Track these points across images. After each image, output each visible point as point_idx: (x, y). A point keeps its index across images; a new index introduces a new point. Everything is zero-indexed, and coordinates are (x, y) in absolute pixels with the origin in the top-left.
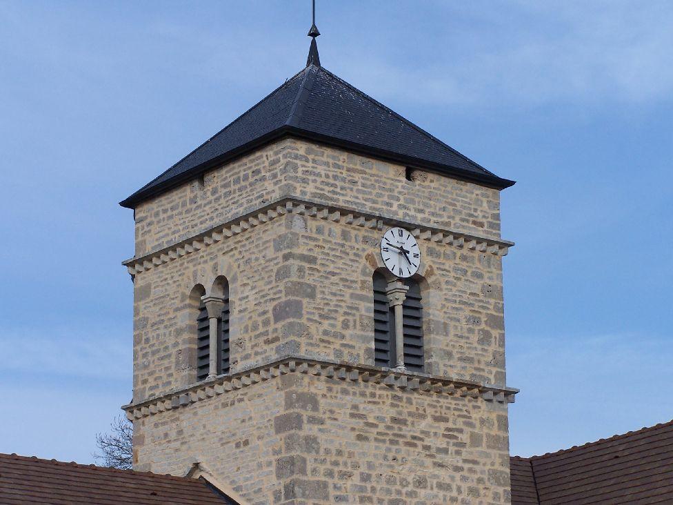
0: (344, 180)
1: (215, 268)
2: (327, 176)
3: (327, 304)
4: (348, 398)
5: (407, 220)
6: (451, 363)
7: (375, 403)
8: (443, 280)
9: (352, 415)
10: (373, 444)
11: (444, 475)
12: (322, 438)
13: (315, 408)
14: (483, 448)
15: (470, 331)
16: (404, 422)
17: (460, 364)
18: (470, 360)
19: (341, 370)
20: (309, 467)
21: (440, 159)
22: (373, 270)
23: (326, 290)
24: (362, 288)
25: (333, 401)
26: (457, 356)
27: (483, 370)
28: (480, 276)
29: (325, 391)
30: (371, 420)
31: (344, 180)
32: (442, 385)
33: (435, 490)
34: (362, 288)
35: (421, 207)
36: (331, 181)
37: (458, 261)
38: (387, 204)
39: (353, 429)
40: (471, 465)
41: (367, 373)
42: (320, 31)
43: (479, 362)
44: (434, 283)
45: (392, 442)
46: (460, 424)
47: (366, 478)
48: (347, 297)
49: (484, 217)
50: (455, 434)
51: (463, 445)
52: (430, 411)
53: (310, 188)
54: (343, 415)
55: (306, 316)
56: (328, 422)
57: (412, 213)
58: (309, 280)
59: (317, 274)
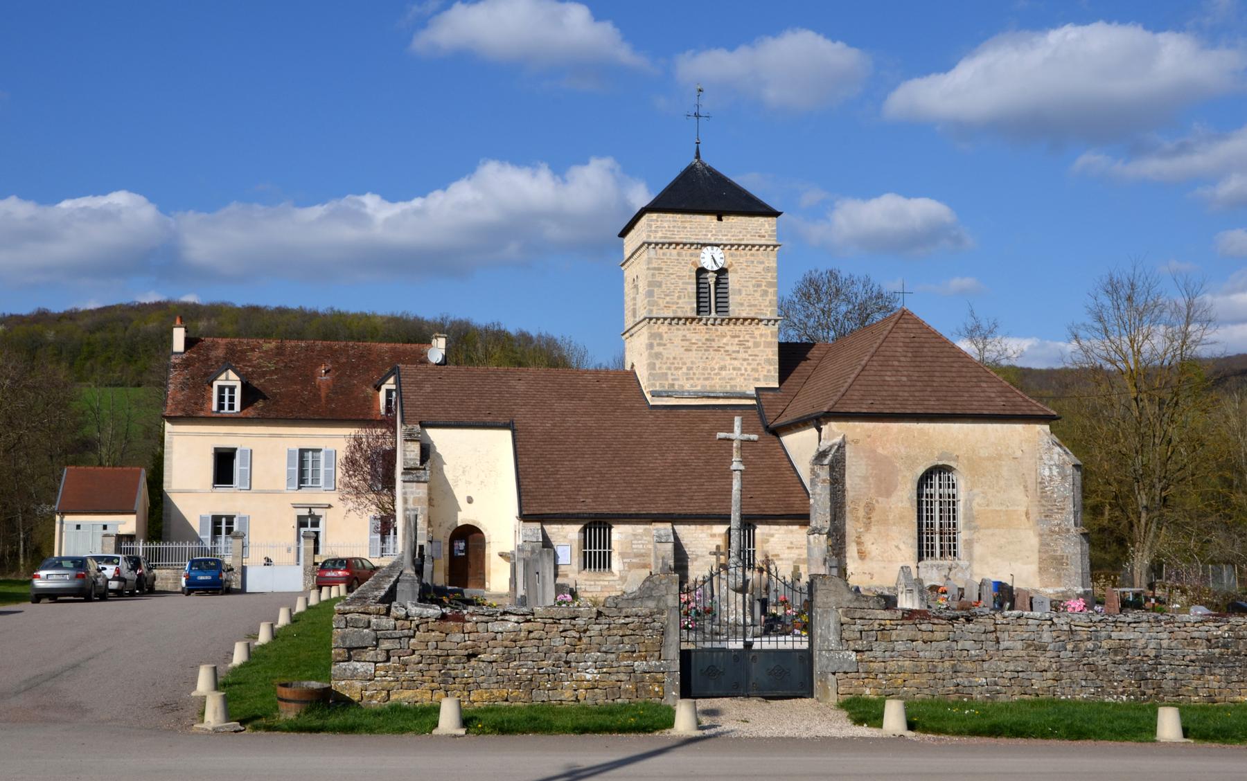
0: (679, 227)
2: (669, 227)
4: (680, 332)
8: (738, 268)
9: (682, 340)
10: (694, 352)
11: (736, 363)
12: (665, 353)
13: (661, 338)
14: (762, 348)
15: (755, 291)
16: (714, 340)
17: (748, 308)
18: (755, 306)
20: (657, 366)
26: (746, 304)
30: (694, 341)
31: (679, 227)
33: (731, 371)
36: (671, 229)
38: (705, 235)
45: (706, 350)
46: (747, 337)
47: (690, 369)
48: (680, 284)
51: (749, 348)
53: (660, 234)
54: (677, 341)
55: (656, 296)
56: (668, 345)
58: (659, 279)
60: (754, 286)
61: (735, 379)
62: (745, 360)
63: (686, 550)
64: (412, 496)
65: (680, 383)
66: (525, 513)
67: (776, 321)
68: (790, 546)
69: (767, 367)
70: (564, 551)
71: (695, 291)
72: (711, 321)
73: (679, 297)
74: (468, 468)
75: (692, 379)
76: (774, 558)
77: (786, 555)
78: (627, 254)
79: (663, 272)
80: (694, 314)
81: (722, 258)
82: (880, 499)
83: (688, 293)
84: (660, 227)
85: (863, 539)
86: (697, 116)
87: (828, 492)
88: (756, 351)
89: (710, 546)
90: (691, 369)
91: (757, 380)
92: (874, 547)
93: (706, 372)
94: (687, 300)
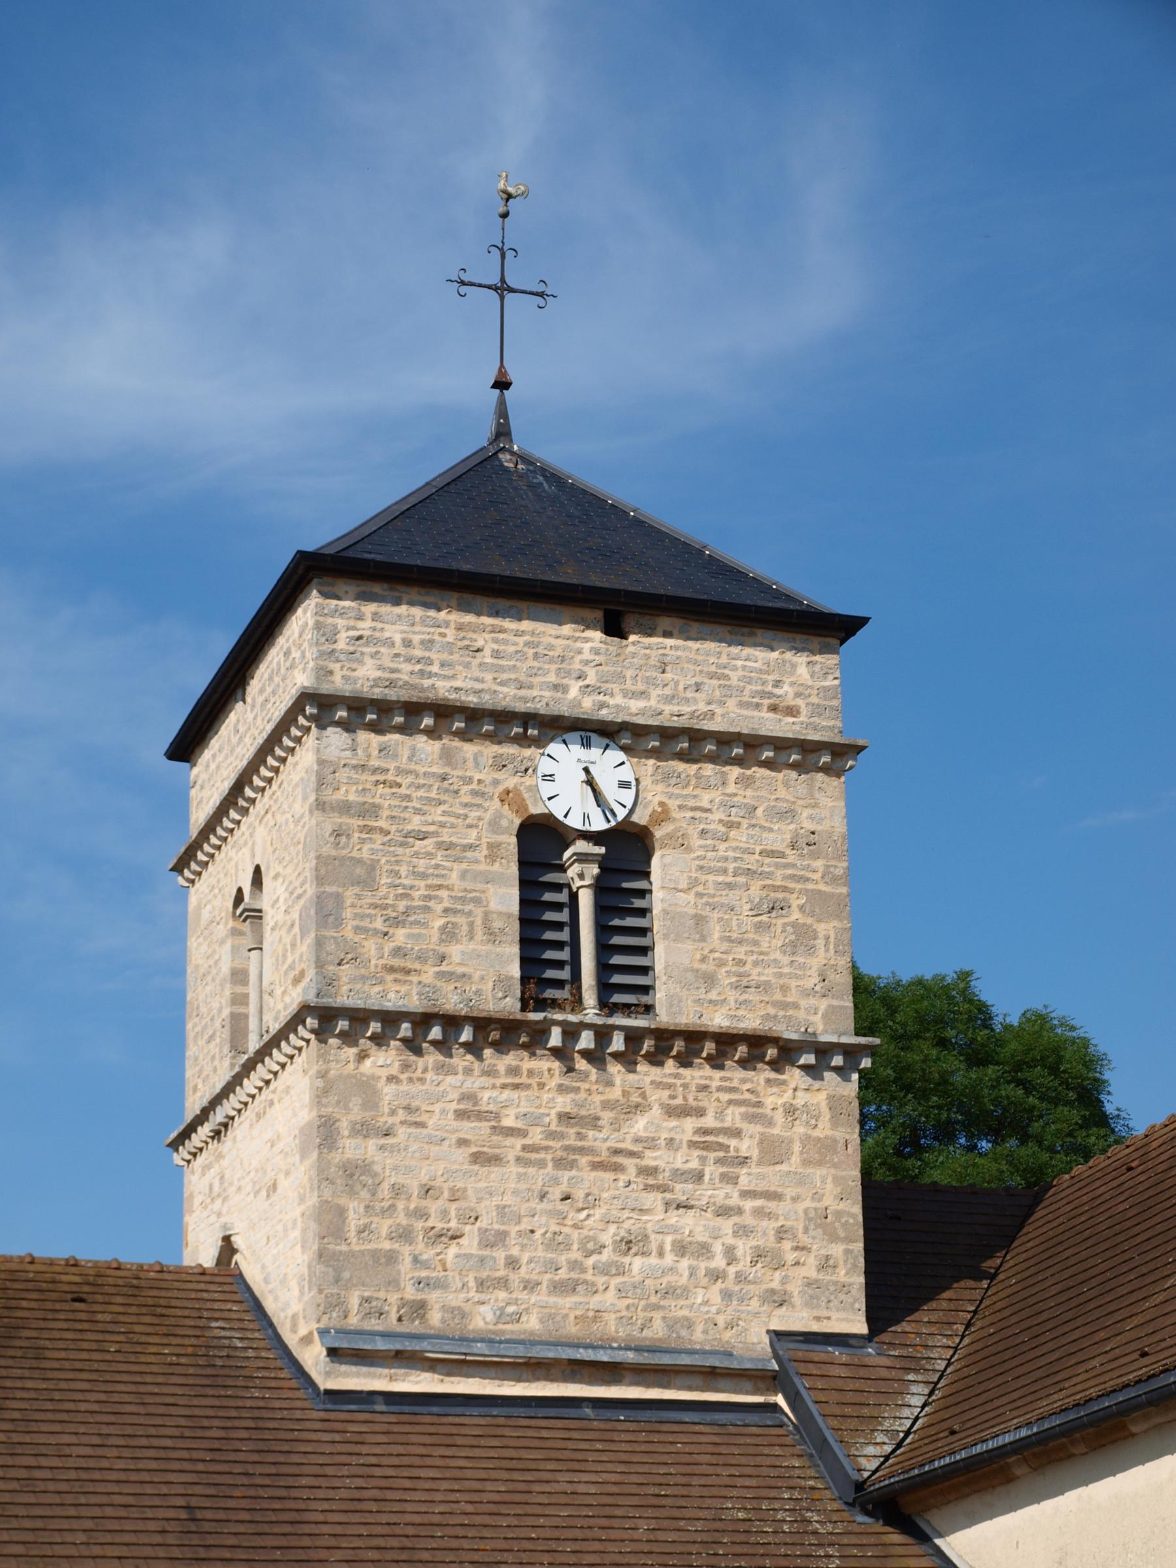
1: (253, 856)
2: (407, 643)
3: (405, 896)
4: (450, 1079)
5: (604, 715)
6: (713, 995)
7: (516, 1087)
8: (693, 832)
9: (461, 1115)
10: (513, 1169)
13: (371, 1100)
15: (759, 927)
16: (594, 1122)
17: (732, 996)
20: (353, 1222)
22: (517, 822)
23: (403, 870)
24: (492, 858)
25: (417, 1088)
26: (725, 979)
27: (796, 1006)
28: (788, 814)
29: (395, 1070)
30: (508, 1122)
33: (669, 1258)
34: (492, 858)
35: (640, 687)
36: (418, 653)
37: (731, 788)
38: (556, 687)
39: (462, 1142)
40: (759, 1203)
42: (513, 375)
43: (784, 989)
44: (670, 836)
45: (559, 1163)
46: (733, 1117)
48: (454, 876)
49: (798, 695)
50: (721, 1139)
51: (744, 1161)
52: (657, 1096)
54: (441, 1118)
55: (350, 924)
56: (402, 1131)
57: (618, 700)
58: (365, 854)
59: (379, 838)
60: (756, 910)
61: (685, 1292)
62: (724, 1212)
65: (455, 1299)
67: (850, 1052)
69: (819, 1247)
71: (515, 908)
72: (586, 1040)
73: (449, 934)
75: (503, 1283)
78: (199, 815)
79: (382, 823)
80: (509, 1005)
81: (624, 785)
83: (486, 914)
84: (370, 641)
86: (502, 289)
88: (771, 1177)
90: (499, 1239)
93: (563, 1259)
94: (478, 945)
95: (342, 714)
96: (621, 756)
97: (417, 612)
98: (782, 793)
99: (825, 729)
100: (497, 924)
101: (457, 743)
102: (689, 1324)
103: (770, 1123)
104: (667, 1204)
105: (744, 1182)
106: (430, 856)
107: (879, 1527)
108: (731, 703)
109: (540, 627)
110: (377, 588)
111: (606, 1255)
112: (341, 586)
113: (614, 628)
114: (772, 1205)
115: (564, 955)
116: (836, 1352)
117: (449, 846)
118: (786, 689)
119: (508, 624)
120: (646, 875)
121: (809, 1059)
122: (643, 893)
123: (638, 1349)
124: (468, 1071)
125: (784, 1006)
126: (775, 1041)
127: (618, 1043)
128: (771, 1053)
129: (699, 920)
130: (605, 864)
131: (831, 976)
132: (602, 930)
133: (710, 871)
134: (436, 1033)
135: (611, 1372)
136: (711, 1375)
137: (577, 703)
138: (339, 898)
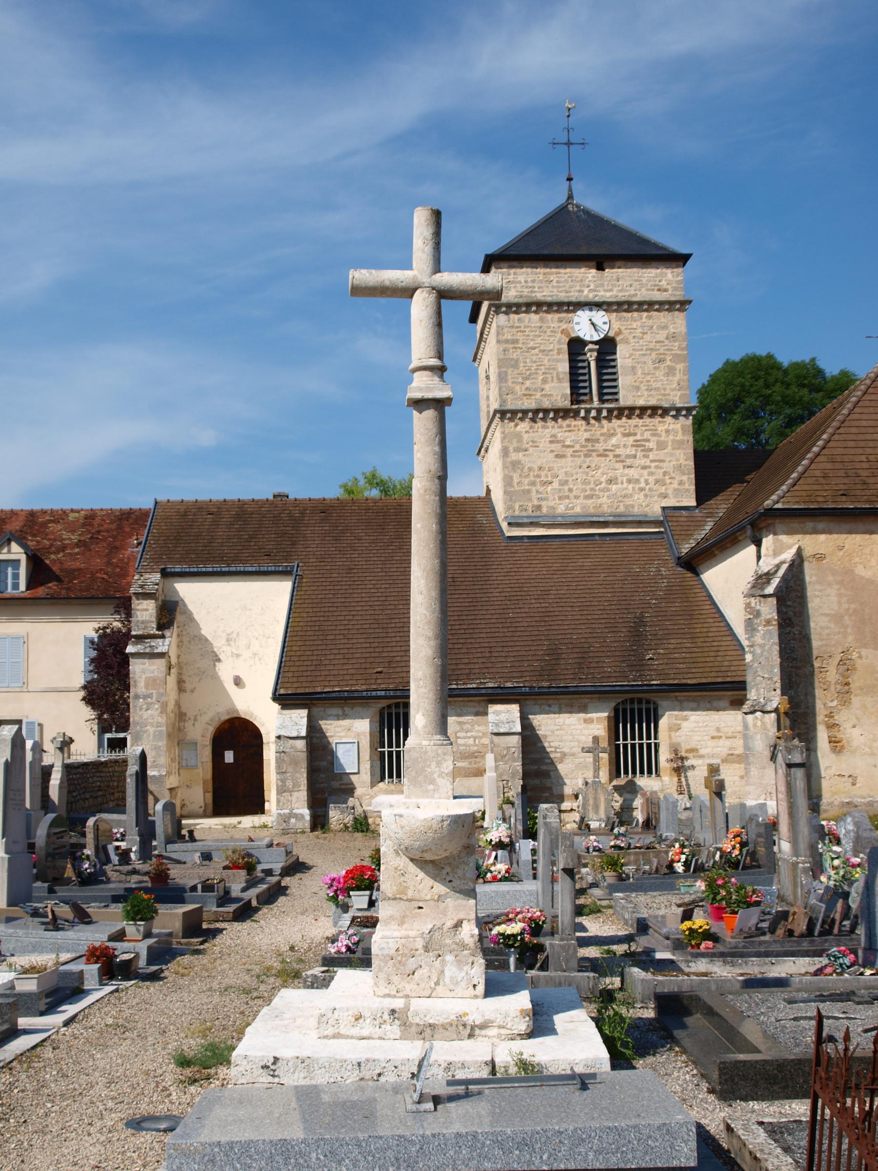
3: (529, 370)
4: (547, 430)
5: (597, 299)
6: (639, 394)
7: (570, 431)
8: (631, 337)
9: (551, 442)
10: (570, 459)
15: (655, 368)
16: (597, 441)
17: (646, 393)
18: (657, 389)
19: (539, 414)
20: (516, 480)
21: (636, 249)
22: (567, 340)
23: (528, 361)
24: (559, 353)
26: (643, 387)
27: (669, 395)
28: (665, 327)
29: (528, 429)
30: (568, 443)
31: (541, 282)
32: (630, 412)
33: (625, 485)
34: (559, 353)
35: (610, 287)
36: (530, 285)
38: (579, 291)
39: (552, 451)
40: (657, 464)
41: (561, 413)
42: (572, 176)
43: (665, 389)
44: (622, 339)
45: (586, 456)
46: (647, 435)
49: (668, 284)
50: (643, 443)
51: (651, 450)
54: (544, 443)
56: (531, 450)
57: (602, 293)
58: (515, 356)
59: (519, 351)
60: (654, 362)
61: (631, 496)
62: (644, 468)
63: (546, 745)
64: (144, 677)
65: (551, 504)
66: (282, 691)
68: (715, 734)
69: (679, 477)
70: (349, 751)
72: (593, 413)
73: (545, 381)
74: (234, 636)
75: (568, 497)
76: (690, 755)
77: (708, 750)
79: (520, 345)
80: (567, 404)
81: (605, 323)
82: (864, 652)
83: (557, 374)
85: (838, 718)
86: (569, 144)
87: (776, 639)
88: (661, 455)
89: (583, 738)
90: (566, 482)
91: (665, 496)
92: (856, 732)
93: (588, 488)
94: (555, 384)
95: (504, 309)
96: (603, 313)
97: (529, 270)
98: (663, 320)
99: (678, 296)
100: (561, 376)
101: (545, 315)
102: (633, 506)
103: (660, 436)
104: (624, 467)
105: (651, 457)
106: (537, 355)
107: (685, 571)
108: (643, 290)
109: (573, 270)
110: (515, 264)
111: (603, 485)
112: (502, 264)
113: (600, 268)
114: (661, 464)
115: (587, 384)
116: (684, 512)
117: (544, 351)
118: (664, 283)
119: (562, 271)
120: (615, 353)
121: (673, 413)
122: (614, 360)
123: (614, 516)
124: (553, 427)
125: (665, 395)
126: (661, 408)
127: (605, 413)
128: (660, 412)
129: (633, 368)
130: (599, 352)
131: (682, 383)
132: (600, 374)
133: (637, 350)
134: (541, 415)
135: (605, 524)
136: (640, 523)
137: (587, 296)
138: (506, 373)
